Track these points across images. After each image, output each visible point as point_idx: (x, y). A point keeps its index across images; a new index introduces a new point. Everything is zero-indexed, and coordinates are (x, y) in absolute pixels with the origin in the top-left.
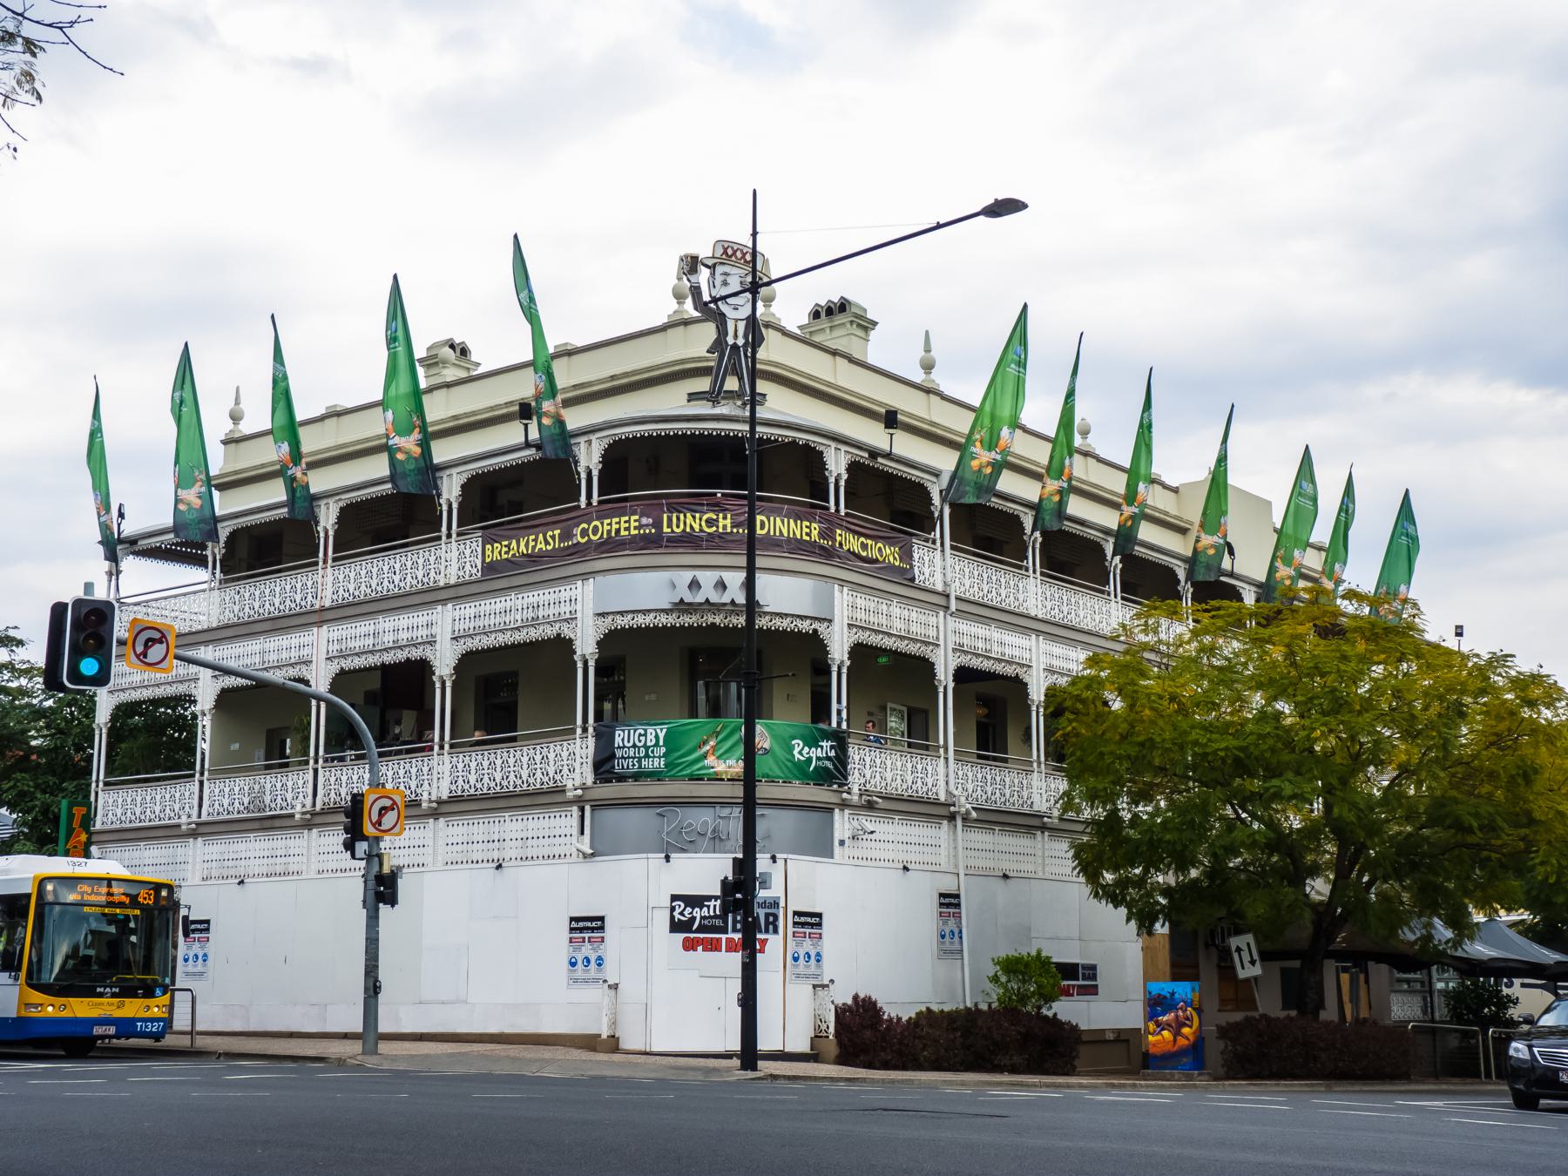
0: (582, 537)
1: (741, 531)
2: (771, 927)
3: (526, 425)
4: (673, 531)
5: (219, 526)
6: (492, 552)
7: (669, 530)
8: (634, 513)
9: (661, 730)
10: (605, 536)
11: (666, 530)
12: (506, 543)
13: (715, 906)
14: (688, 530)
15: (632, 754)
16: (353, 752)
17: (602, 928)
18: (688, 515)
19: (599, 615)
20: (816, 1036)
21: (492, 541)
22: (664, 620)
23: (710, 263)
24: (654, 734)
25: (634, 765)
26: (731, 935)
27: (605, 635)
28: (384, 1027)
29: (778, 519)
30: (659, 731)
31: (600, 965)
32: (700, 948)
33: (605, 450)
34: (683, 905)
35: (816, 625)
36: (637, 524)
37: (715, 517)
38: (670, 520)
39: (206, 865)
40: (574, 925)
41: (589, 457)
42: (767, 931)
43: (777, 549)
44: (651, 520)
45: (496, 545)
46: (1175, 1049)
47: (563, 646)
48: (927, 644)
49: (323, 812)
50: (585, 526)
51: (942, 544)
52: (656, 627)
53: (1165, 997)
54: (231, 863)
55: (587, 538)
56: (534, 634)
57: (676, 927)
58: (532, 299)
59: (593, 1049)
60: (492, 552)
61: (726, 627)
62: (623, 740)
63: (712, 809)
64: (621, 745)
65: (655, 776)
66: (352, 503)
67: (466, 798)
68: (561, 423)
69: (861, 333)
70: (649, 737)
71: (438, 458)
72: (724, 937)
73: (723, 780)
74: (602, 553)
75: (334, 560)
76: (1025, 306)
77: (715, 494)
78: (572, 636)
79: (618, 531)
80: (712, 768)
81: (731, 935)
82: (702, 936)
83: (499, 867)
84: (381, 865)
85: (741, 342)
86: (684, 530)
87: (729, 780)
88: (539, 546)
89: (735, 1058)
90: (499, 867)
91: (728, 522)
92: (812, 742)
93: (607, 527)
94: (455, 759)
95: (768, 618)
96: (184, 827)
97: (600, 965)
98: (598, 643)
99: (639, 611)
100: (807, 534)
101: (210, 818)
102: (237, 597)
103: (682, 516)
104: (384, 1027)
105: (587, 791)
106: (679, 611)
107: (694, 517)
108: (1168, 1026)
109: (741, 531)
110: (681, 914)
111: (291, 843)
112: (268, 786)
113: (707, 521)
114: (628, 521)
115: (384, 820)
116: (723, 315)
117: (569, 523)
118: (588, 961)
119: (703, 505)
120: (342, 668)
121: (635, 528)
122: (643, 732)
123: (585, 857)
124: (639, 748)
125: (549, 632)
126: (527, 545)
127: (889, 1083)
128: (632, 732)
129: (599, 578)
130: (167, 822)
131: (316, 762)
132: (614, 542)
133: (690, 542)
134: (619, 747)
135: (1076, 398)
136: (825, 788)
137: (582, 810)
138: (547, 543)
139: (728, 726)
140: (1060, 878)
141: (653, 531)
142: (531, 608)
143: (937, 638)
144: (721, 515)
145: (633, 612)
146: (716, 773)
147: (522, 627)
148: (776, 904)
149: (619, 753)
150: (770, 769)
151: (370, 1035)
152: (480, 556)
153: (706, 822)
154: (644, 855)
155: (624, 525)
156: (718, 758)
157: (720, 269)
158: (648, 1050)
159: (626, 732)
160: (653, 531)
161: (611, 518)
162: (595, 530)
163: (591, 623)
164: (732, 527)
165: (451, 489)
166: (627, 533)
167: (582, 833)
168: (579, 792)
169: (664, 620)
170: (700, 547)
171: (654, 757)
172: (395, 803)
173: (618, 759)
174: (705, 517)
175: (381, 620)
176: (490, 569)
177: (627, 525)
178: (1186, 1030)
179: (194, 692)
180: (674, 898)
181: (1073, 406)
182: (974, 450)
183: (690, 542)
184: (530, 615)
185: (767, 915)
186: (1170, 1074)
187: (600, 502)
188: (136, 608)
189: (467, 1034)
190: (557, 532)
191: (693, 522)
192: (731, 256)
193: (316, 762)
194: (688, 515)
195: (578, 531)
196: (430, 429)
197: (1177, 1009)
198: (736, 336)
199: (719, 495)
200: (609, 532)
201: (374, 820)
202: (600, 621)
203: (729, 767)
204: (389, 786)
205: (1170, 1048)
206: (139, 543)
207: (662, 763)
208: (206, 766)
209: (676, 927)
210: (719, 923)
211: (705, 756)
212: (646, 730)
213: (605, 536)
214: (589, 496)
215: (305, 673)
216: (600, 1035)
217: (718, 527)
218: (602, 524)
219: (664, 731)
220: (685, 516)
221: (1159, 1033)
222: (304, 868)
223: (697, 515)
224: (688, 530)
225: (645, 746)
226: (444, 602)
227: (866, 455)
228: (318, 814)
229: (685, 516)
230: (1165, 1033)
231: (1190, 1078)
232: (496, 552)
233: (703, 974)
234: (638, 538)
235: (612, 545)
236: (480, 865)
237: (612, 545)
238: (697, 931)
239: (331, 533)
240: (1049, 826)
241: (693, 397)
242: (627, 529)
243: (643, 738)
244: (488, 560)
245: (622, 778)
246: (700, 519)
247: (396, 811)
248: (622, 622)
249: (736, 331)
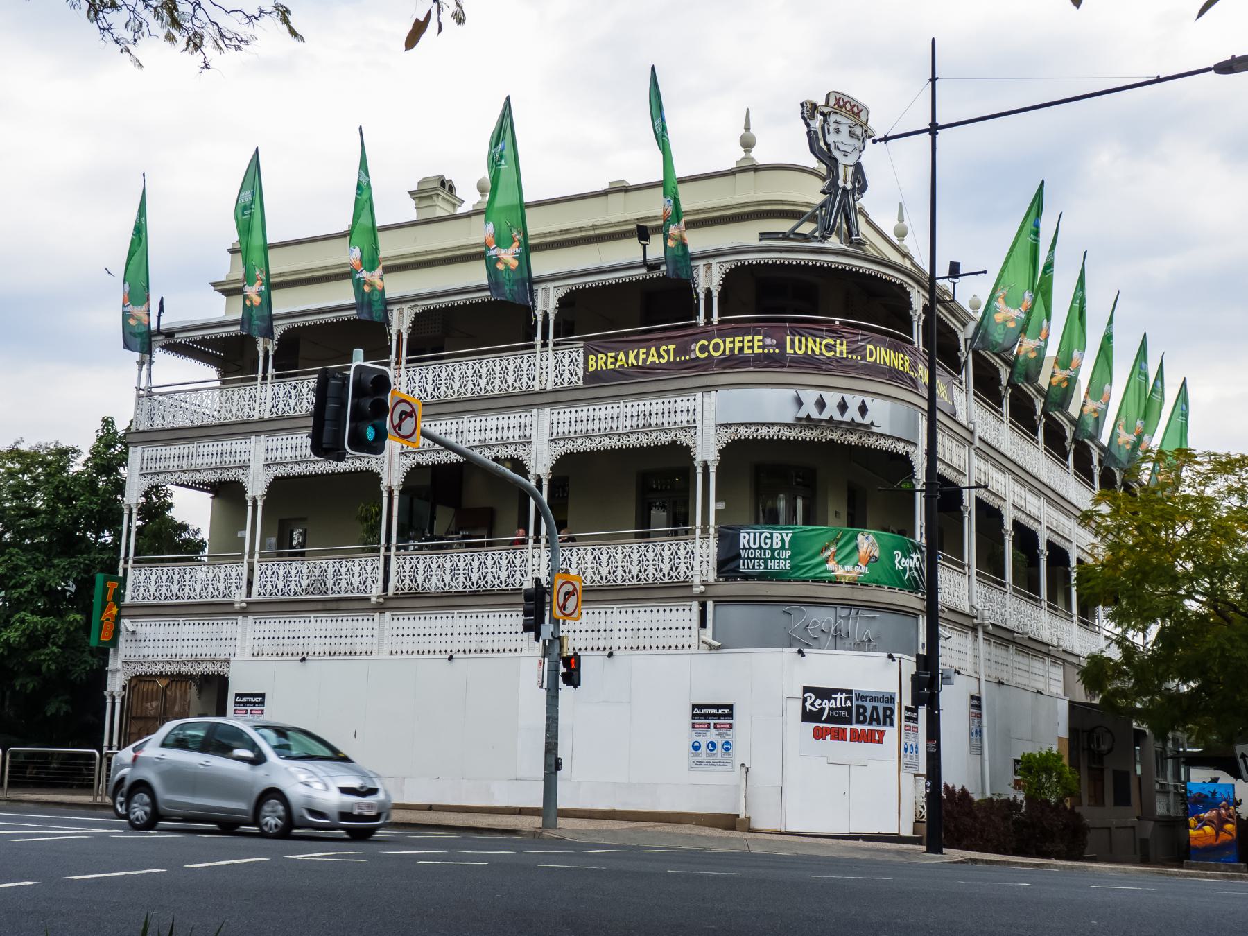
0: (702, 352)
1: (854, 357)
2: (888, 720)
3: (644, 246)
4: (795, 353)
5: (275, 323)
6: (597, 361)
7: (792, 351)
8: (758, 333)
9: (787, 534)
10: (727, 353)
11: (789, 351)
12: (613, 354)
13: (841, 699)
14: (809, 352)
15: (758, 555)
16: (417, 543)
17: (730, 716)
18: (810, 339)
19: (721, 425)
20: (917, 822)
21: (596, 352)
22: (787, 434)
23: (826, 110)
24: (780, 538)
25: (760, 566)
26: (854, 726)
27: (728, 444)
28: (563, 803)
29: (882, 349)
30: (784, 535)
31: (727, 749)
32: (828, 737)
33: (726, 274)
35: (908, 448)
36: (761, 344)
37: (833, 343)
38: (792, 342)
39: (256, 642)
40: (697, 711)
41: (709, 279)
42: (885, 724)
43: (882, 376)
44: (774, 341)
45: (600, 356)
46: (1218, 842)
47: (681, 454)
48: (960, 472)
49: (396, 597)
50: (706, 343)
52: (779, 440)
53: (1206, 796)
54: (286, 641)
55: (706, 354)
56: (644, 440)
57: (808, 716)
58: (664, 129)
59: (734, 829)
60: (597, 361)
61: (842, 444)
62: (749, 542)
63: (834, 610)
64: (747, 546)
65: (779, 577)
66: (429, 309)
67: (596, 588)
68: (684, 246)
70: (775, 540)
71: (536, 272)
72: (848, 727)
73: (841, 583)
74: (724, 368)
75: (408, 362)
76: (1043, 182)
77: (834, 322)
78: (690, 444)
79: (741, 349)
80: (833, 571)
81: (854, 726)
82: (830, 726)
83: (303, 660)
84: (561, 647)
85: (849, 186)
86: (806, 353)
87: (846, 583)
88: (650, 359)
89: (860, 840)
90: (303, 660)
91: (844, 348)
92: (906, 554)
93: (729, 345)
94: (229, 568)
95: (875, 438)
96: (237, 605)
97: (727, 749)
98: (720, 451)
99: (763, 424)
100: (902, 366)
101: (261, 598)
102: (293, 392)
103: (803, 339)
104: (563, 803)
105: (710, 588)
106: (802, 426)
107: (815, 341)
108: (1209, 822)
109: (854, 357)
110: (812, 704)
111: (359, 624)
112: (331, 570)
113: (826, 346)
114: (752, 341)
115: (567, 604)
116: (836, 160)
117: (686, 339)
118: (714, 745)
119: (822, 330)
120: (418, 463)
121: (759, 347)
122: (769, 536)
123: (711, 649)
124: (765, 550)
125: (663, 439)
126: (637, 357)
127: (1068, 869)
128: (758, 535)
129: (721, 392)
130: (209, 599)
131: (388, 549)
132: (735, 360)
133: (810, 363)
134: (745, 548)
135: (1055, 273)
136: (914, 594)
137: (703, 606)
138: (660, 356)
139: (846, 534)
140: (1023, 687)
141: (777, 351)
142: (642, 416)
143: (965, 470)
144: (838, 342)
145: (757, 424)
146: (836, 577)
147: (632, 433)
148: (892, 699)
149: (744, 554)
150: (879, 576)
151: (549, 809)
152: (581, 365)
153: (828, 621)
154: (780, 649)
155: (747, 344)
156: (838, 563)
157: (833, 118)
158: (783, 830)
159: (752, 535)
160: (777, 351)
161: (734, 336)
162: (717, 347)
163: (713, 432)
164: (848, 353)
165: (547, 302)
166: (750, 351)
167: (703, 624)
168: (703, 588)
169: (786, 433)
170: (821, 369)
171: (780, 559)
172: (575, 589)
173: (744, 559)
174: (824, 342)
175: (621, 404)
176: (593, 378)
177: (751, 344)
178: (1229, 827)
179: (243, 479)
180: (806, 690)
181: (1051, 277)
182: (998, 305)
183: (810, 363)
184: (641, 421)
185: (885, 709)
186: (1215, 865)
187: (720, 322)
188: (161, 398)
189: (575, 810)
190: (672, 347)
191: (814, 346)
192: (841, 107)
193: (388, 549)
194: (810, 339)
195: (696, 347)
196: (530, 242)
197: (1220, 808)
198: (845, 182)
199: (837, 323)
200: (732, 349)
201: (561, 604)
202: (722, 431)
203: (848, 572)
204: (573, 572)
205: (1212, 841)
206: (176, 336)
207: (788, 565)
208: (257, 548)
209: (808, 716)
210: (844, 714)
211: (826, 561)
212: (772, 534)
213: (727, 353)
214: (708, 314)
215: (374, 465)
216: (738, 815)
217: (835, 352)
218: (724, 342)
219: (790, 535)
220: (806, 340)
221: (1200, 828)
222: (375, 649)
223: (818, 340)
224: (809, 352)
225: (771, 548)
226: (541, 406)
228: (391, 598)
229: (806, 340)
230: (1207, 828)
231: (1237, 869)
232: (601, 362)
233: (829, 761)
234: (762, 356)
235: (735, 362)
236: (468, 655)
237: (735, 362)
238: (826, 721)
239: (405, 336)
240: (1017, 641)
241: (764, 236)
242: (751, 348)
243: (769, 541)
244: (591, 369)
245: (747, 577)
246: (820, 344)
247: (576, 596)
248: (744, 433)
249: (845, 176)
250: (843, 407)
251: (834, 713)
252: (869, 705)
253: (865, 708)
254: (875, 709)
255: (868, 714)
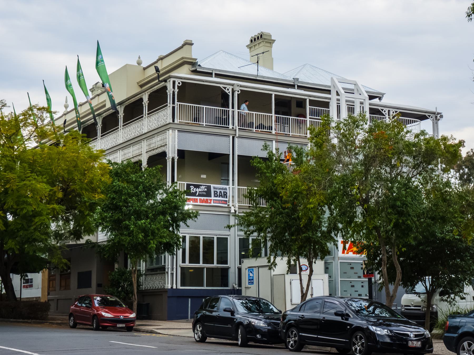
34: (193, 187)
69: (268, 45)
110: (193, 190)
251: (200, 193)
252: (218, 191)
253: (217, 192)
254: (220, 192)
255: (218, 194)
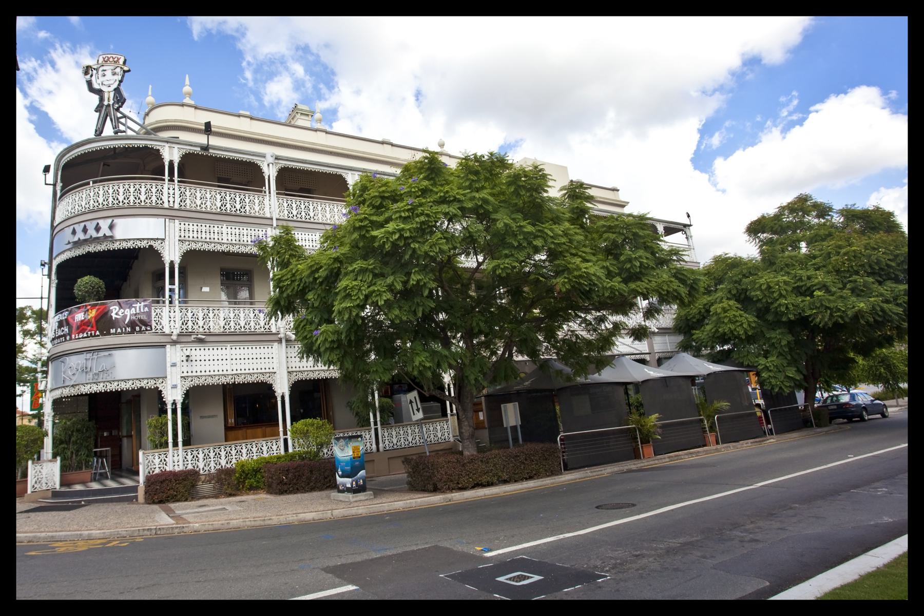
51: (270, 193)
95: (118, 243)
227: (199, 149)
250: (85, 230)
